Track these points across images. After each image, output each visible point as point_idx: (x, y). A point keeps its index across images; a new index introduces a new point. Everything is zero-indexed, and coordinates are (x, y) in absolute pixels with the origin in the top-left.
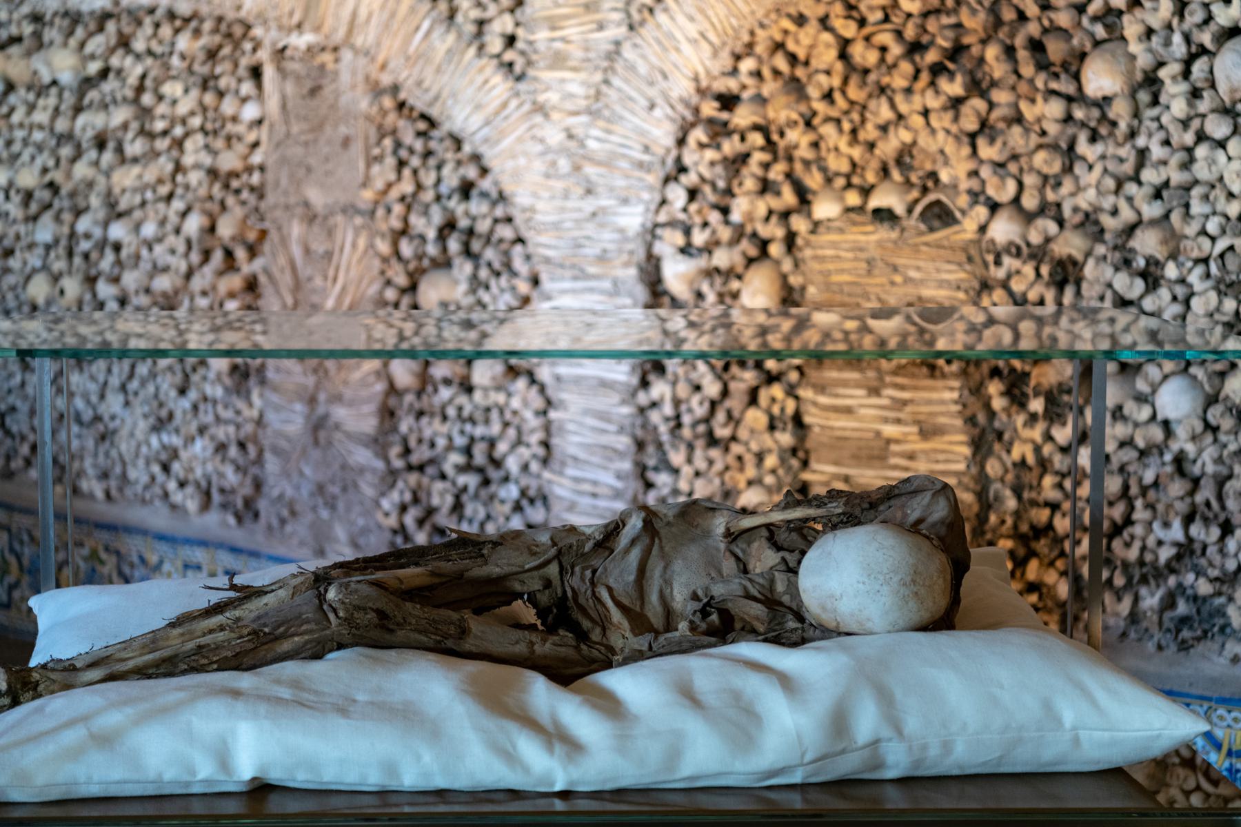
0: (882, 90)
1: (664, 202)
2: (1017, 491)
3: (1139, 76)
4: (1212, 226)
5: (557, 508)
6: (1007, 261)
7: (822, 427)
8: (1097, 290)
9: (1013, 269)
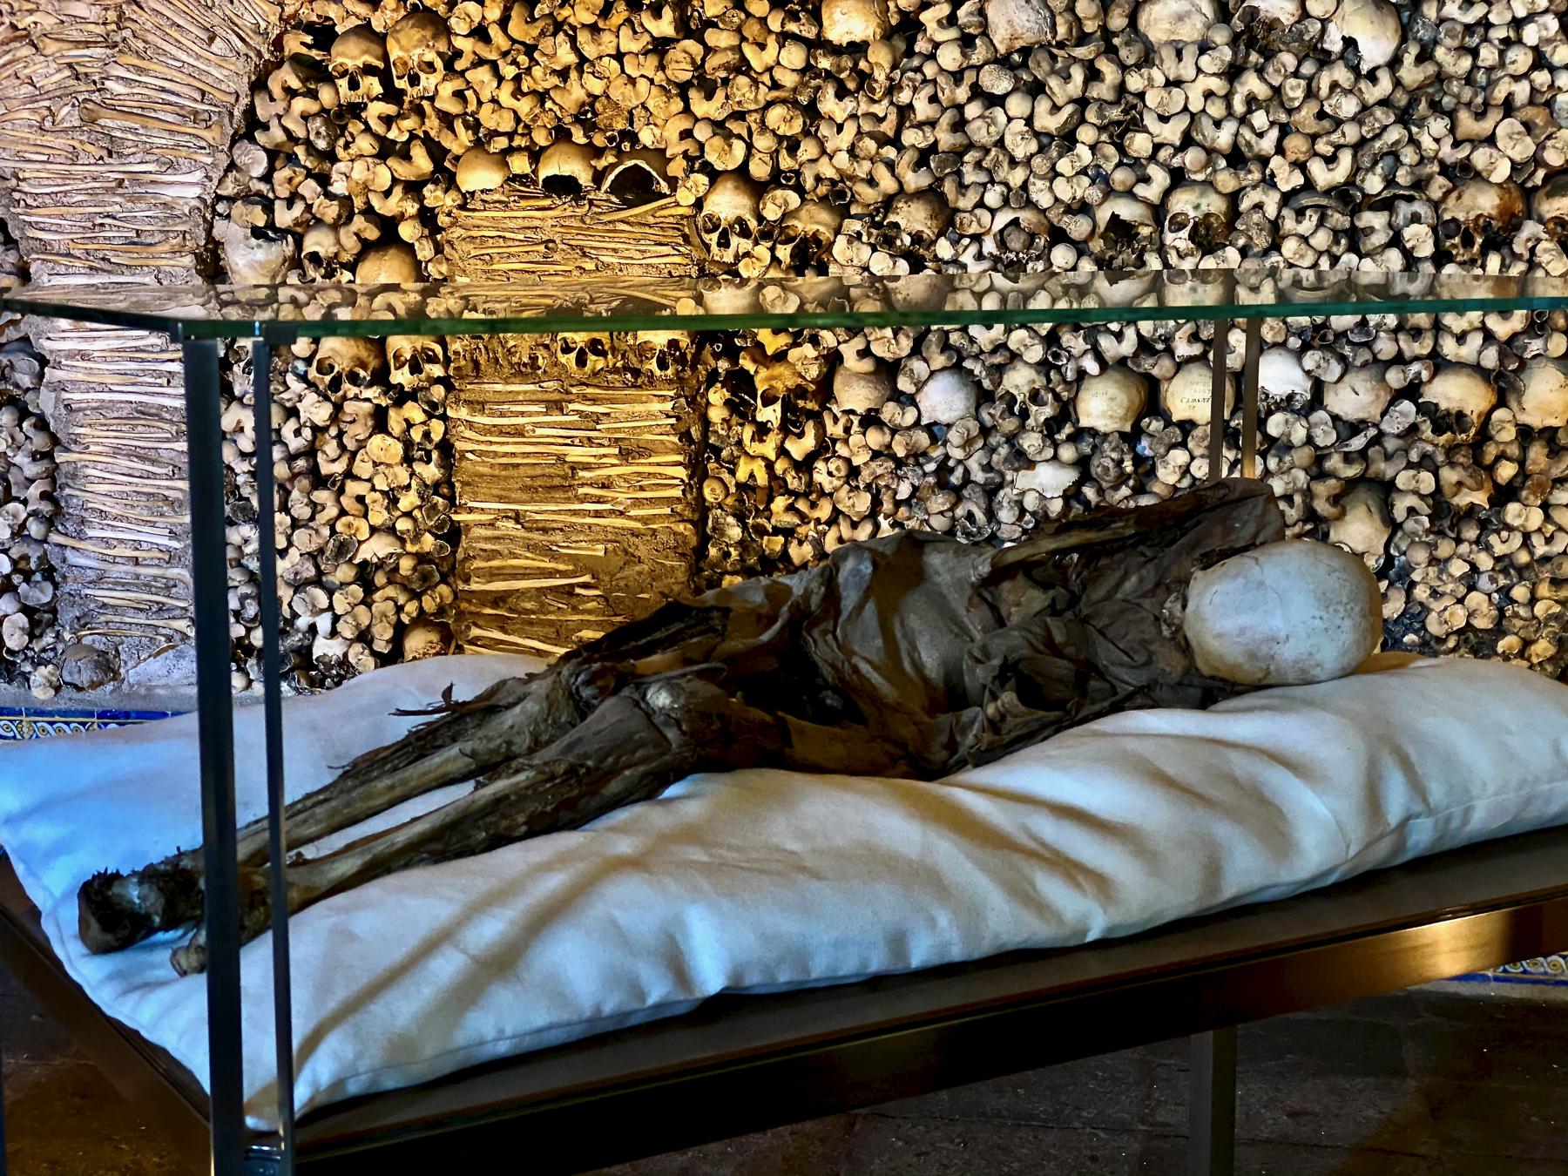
0: (558, 27)
1: (232, 166)
2: (741, 518)
4: (993, 197)
7: (482, 454)
9: (741, 252)
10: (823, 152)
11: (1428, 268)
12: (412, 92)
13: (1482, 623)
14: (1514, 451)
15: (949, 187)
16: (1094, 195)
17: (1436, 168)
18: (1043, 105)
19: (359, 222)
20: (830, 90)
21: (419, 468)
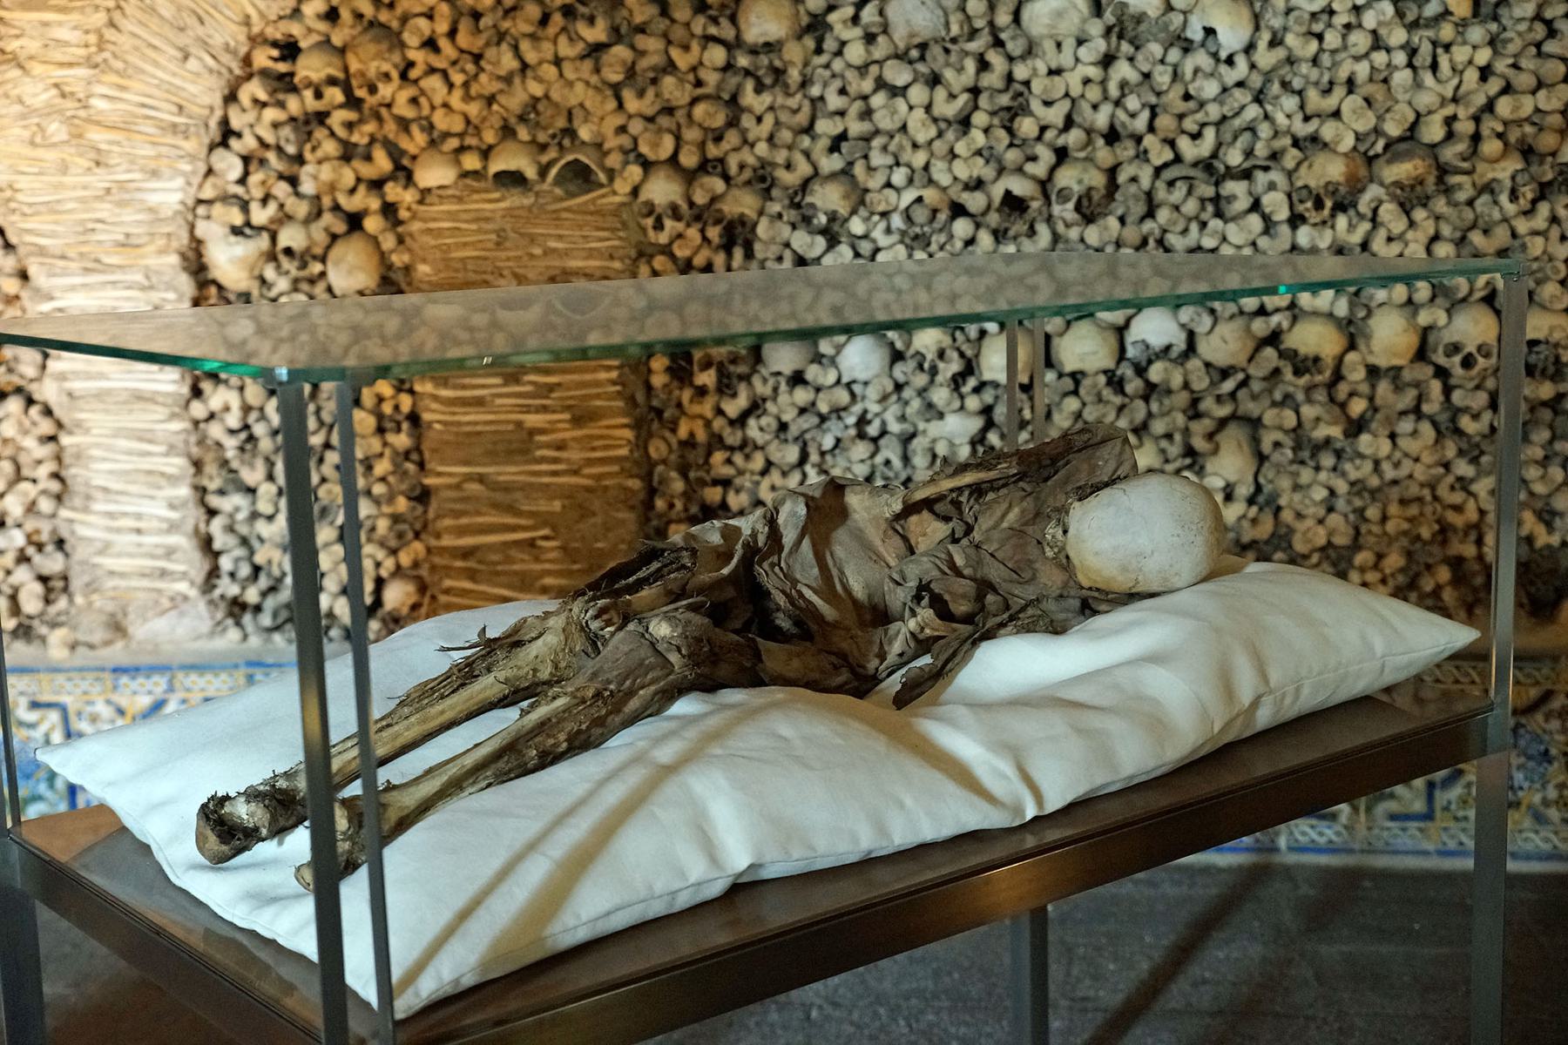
0: (501, 36)
1: (210, 172)
2: (684, 472)
3: (805, 20)
4: (899, 177)
5: (80, 553)
6: (669, 223)
8: (774, 250)
10: (745, 141)
11: (1285, 230)
12: (371, 101)
13: (1341, 540)
14: (1364, 388)
15: (859, 169)
16: (988, 172)
17: (1288, 141)
18: (940, 93)
19: (328, 218)
20: (749, 85)
21: (391, 438)
